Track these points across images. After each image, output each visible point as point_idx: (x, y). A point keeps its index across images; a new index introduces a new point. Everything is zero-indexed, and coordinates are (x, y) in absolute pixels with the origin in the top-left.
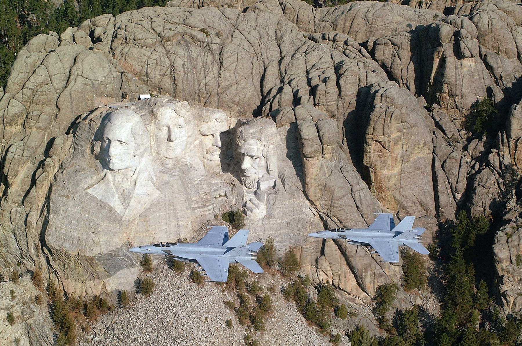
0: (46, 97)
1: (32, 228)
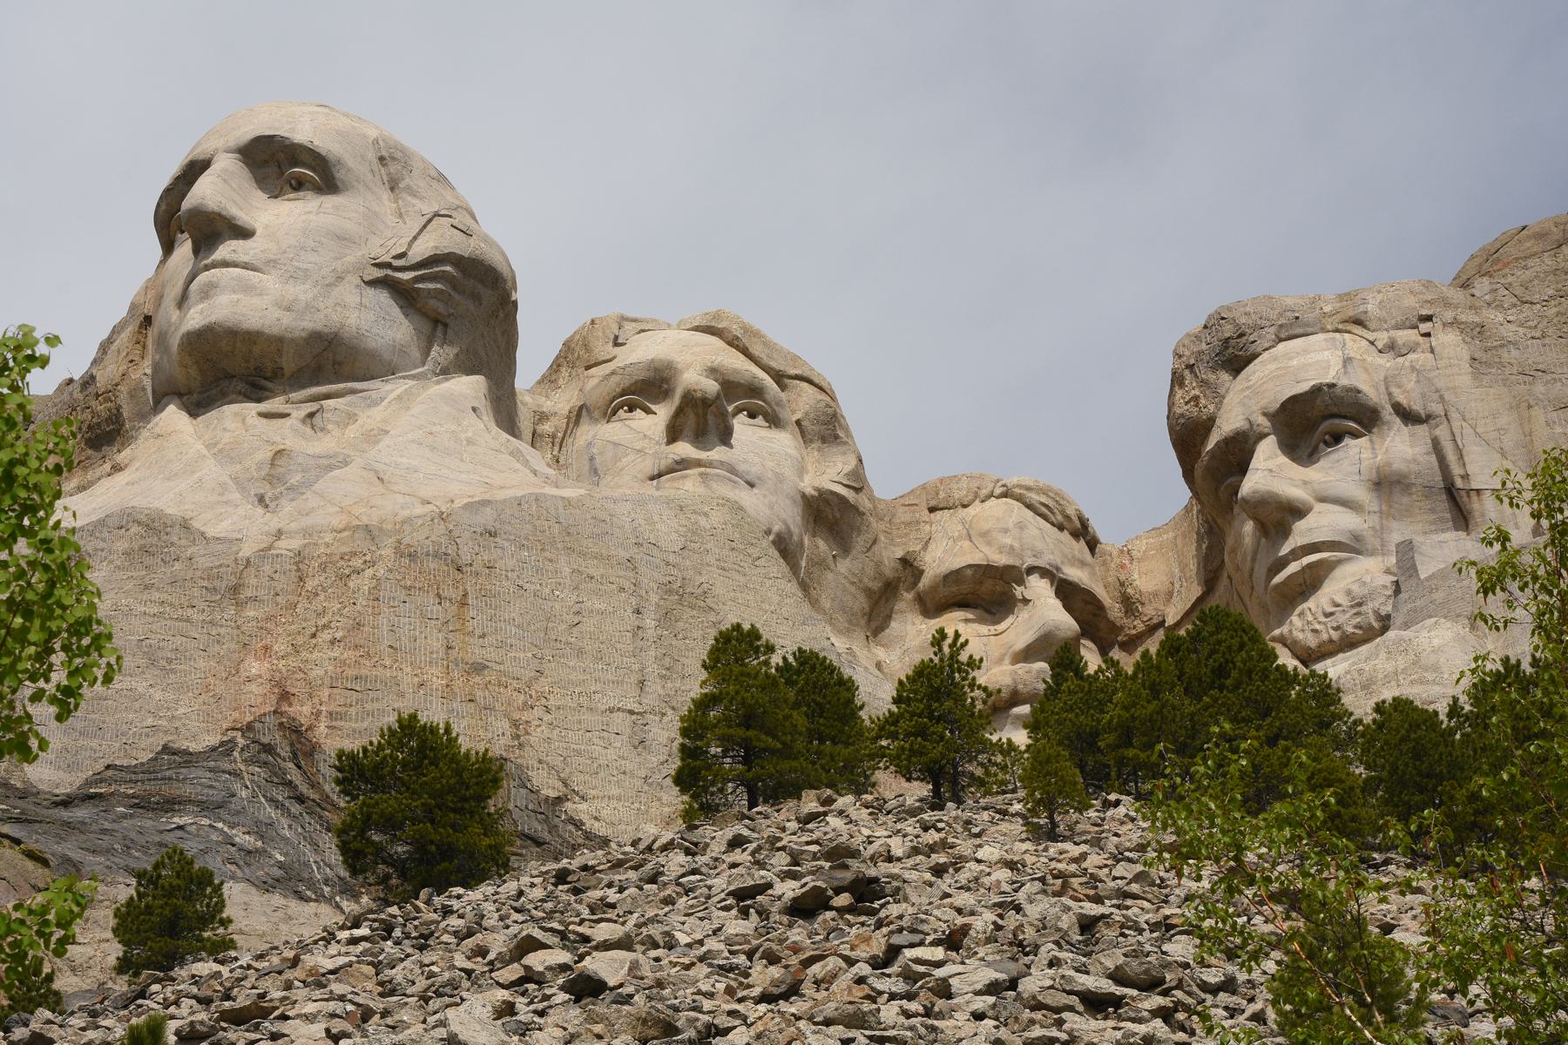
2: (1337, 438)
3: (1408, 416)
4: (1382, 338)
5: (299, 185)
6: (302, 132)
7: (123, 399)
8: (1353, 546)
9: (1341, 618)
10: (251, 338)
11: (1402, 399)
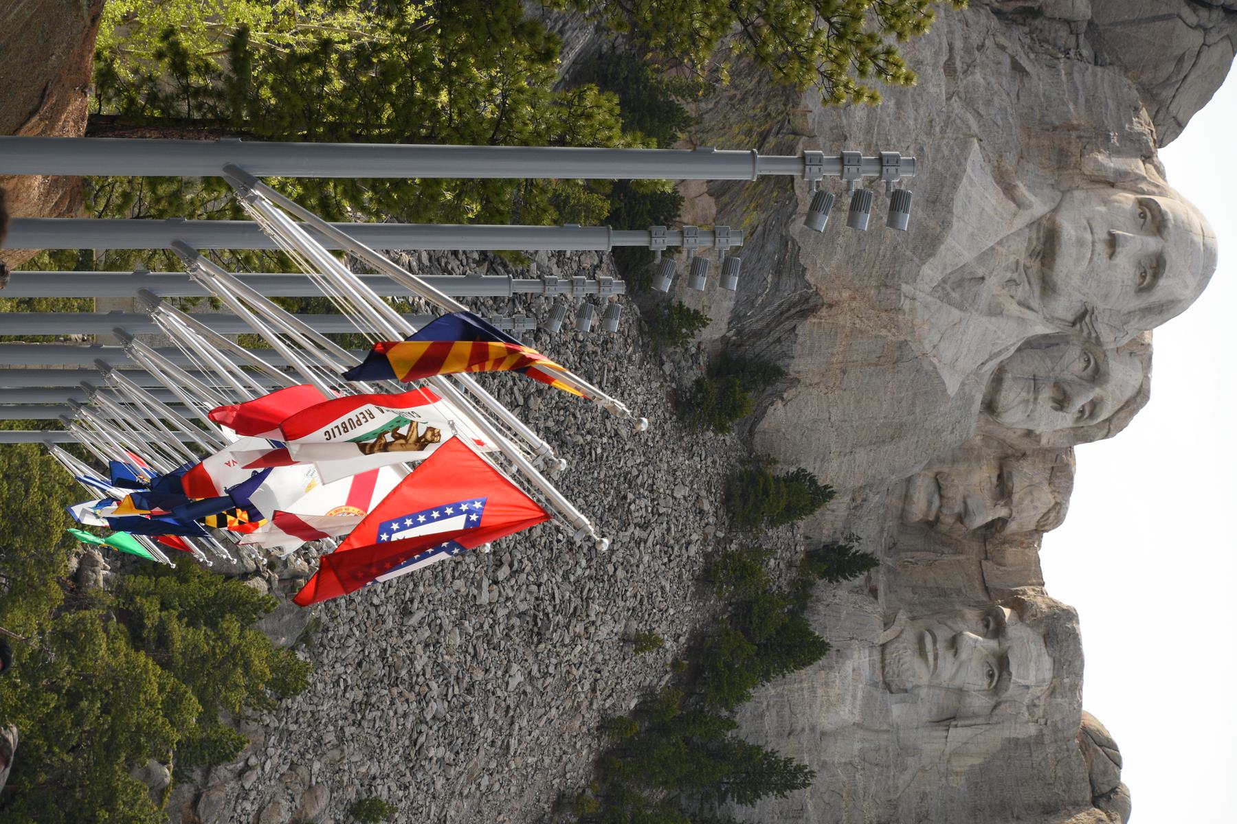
2: (991, 676)
3: (995, 707)
4: (1041, 703)
6: (1162, 282)
8: (935, 672)
10: (1053, 260)
11: (1002, 706)
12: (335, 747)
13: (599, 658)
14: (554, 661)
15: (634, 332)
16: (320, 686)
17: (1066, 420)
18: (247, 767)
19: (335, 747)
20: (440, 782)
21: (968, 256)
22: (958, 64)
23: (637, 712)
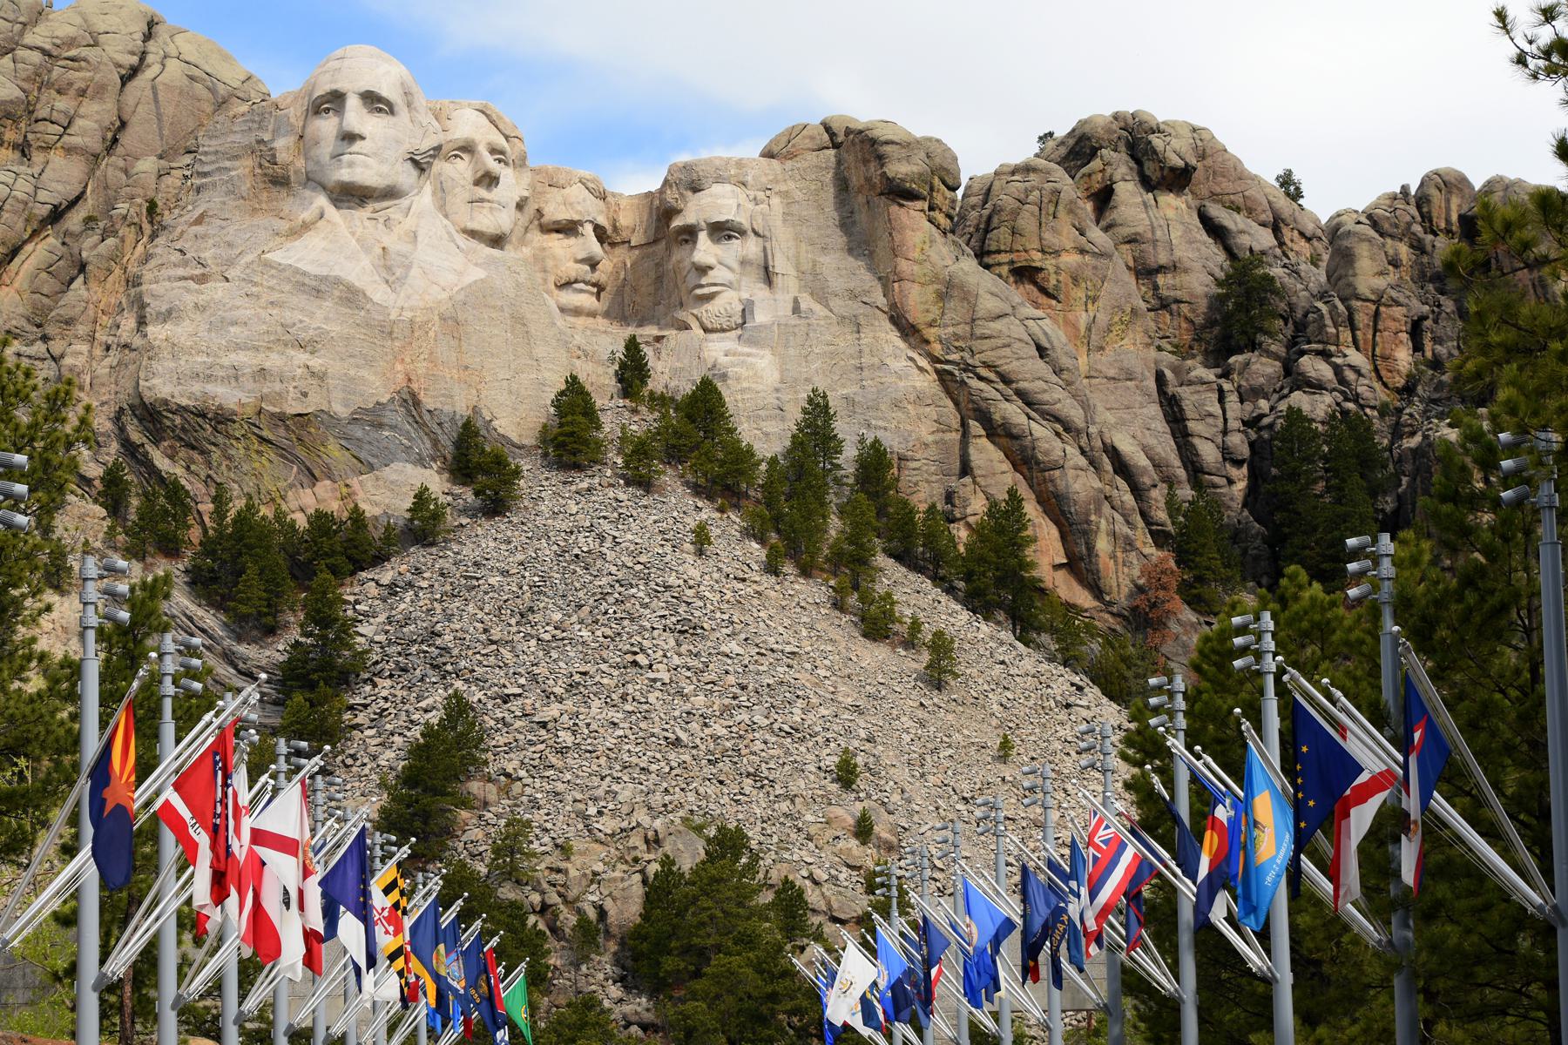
0: (88, 74)
1: (81, 388)
2: (730, 237)
3: (756, 233)
4: (752, 194)
5: (380, 110)
6: (385, 93)
7: (291, 173)
8: (729, 286)
9: (722, 320)
12: (793, 801)
13: (716, 576)
14: (718, 615)
15: (434, 550)
16: (740, 816)
17: (506, 174)
18: (811, 877)
19: (793, 801)
20: (823, 711)
21: (366, 262)
22: (199, 271)
23: (762, 541)
